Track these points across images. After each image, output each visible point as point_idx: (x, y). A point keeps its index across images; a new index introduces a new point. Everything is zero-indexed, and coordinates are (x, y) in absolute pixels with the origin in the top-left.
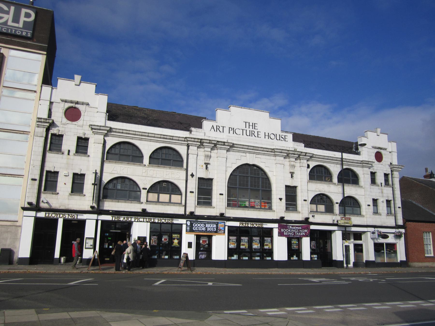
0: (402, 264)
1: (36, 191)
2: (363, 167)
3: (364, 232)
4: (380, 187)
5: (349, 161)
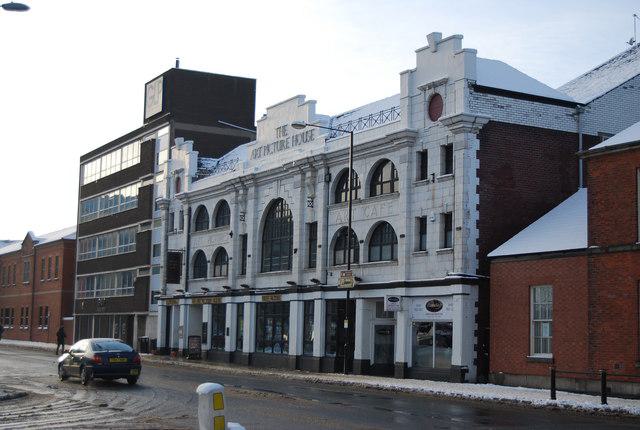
2: (399, 147)
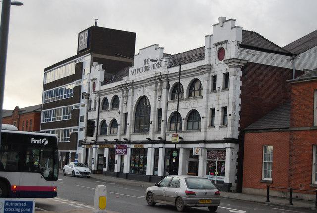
2: (203, 73)
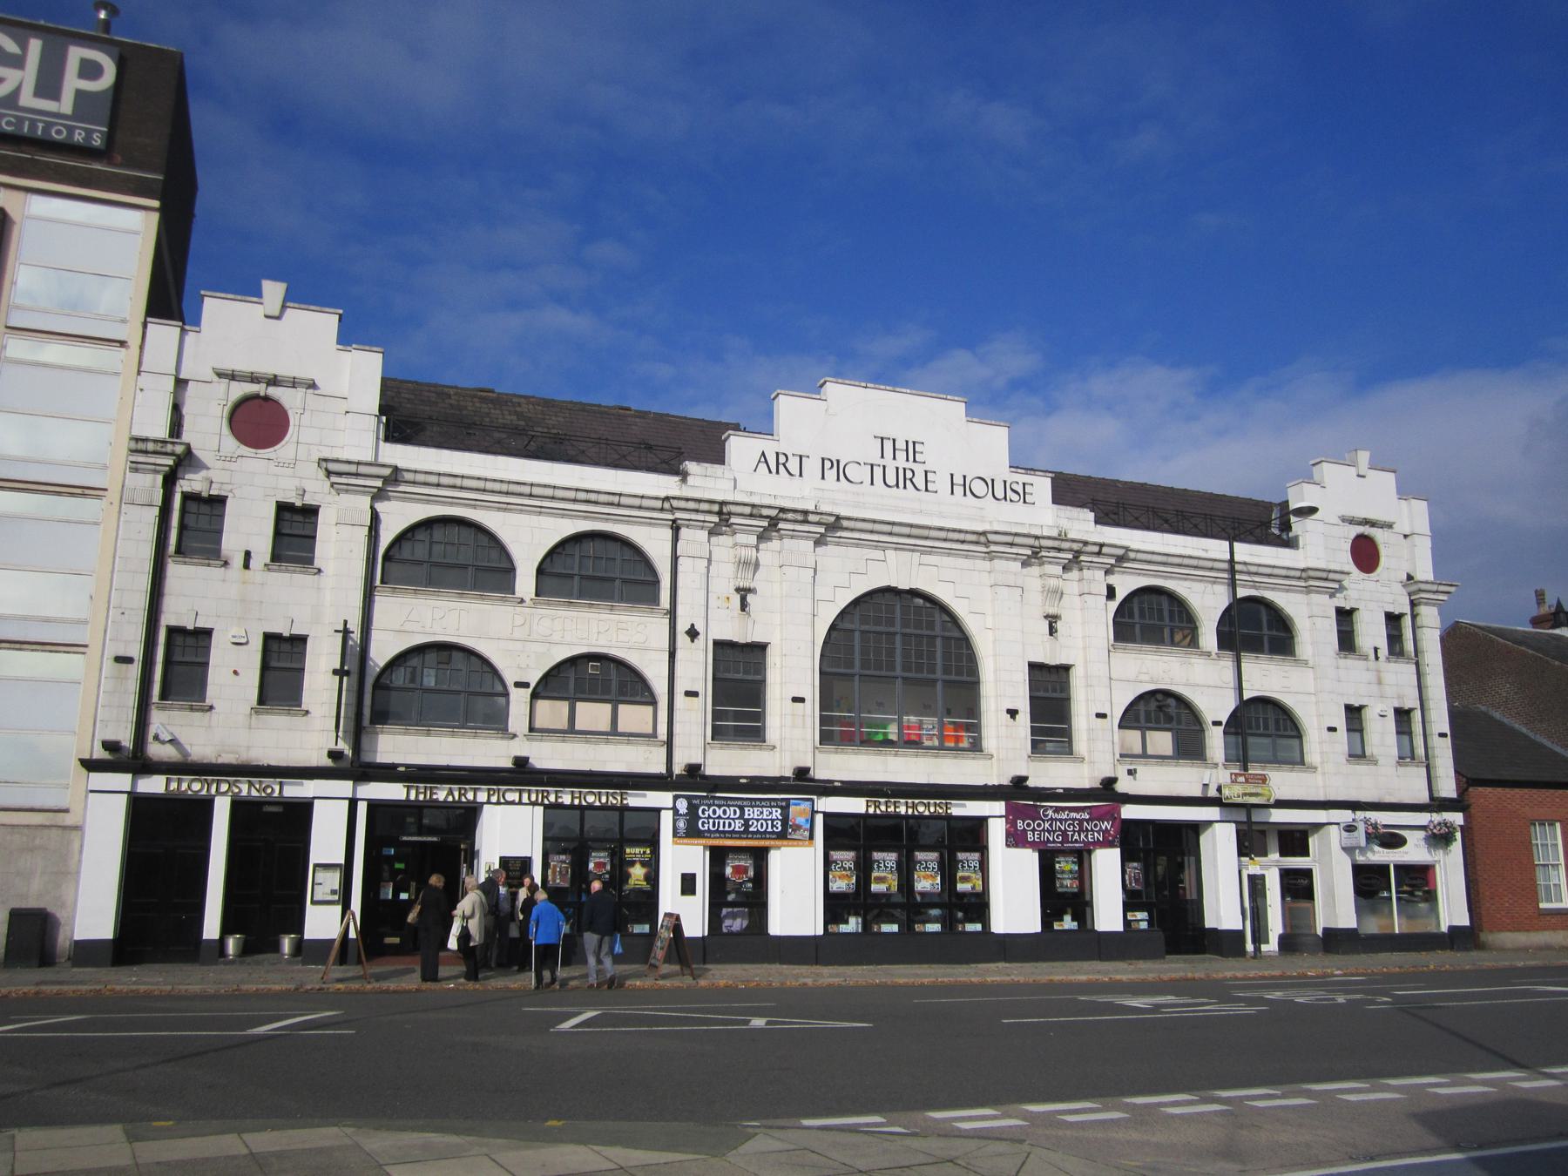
0: (1457, 938)
1: (132, 700)
2: (1308, 590)
3: (1318, 827)
4: (1372, 663)
5: (1256, 571)
